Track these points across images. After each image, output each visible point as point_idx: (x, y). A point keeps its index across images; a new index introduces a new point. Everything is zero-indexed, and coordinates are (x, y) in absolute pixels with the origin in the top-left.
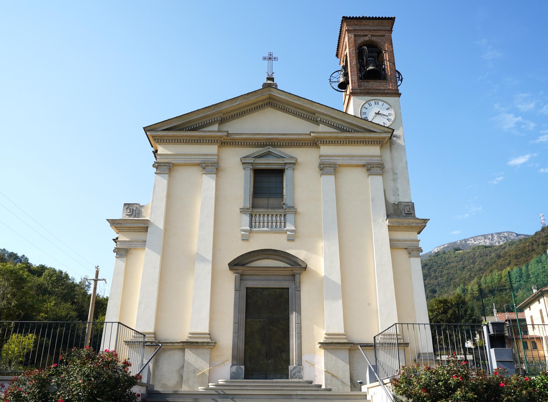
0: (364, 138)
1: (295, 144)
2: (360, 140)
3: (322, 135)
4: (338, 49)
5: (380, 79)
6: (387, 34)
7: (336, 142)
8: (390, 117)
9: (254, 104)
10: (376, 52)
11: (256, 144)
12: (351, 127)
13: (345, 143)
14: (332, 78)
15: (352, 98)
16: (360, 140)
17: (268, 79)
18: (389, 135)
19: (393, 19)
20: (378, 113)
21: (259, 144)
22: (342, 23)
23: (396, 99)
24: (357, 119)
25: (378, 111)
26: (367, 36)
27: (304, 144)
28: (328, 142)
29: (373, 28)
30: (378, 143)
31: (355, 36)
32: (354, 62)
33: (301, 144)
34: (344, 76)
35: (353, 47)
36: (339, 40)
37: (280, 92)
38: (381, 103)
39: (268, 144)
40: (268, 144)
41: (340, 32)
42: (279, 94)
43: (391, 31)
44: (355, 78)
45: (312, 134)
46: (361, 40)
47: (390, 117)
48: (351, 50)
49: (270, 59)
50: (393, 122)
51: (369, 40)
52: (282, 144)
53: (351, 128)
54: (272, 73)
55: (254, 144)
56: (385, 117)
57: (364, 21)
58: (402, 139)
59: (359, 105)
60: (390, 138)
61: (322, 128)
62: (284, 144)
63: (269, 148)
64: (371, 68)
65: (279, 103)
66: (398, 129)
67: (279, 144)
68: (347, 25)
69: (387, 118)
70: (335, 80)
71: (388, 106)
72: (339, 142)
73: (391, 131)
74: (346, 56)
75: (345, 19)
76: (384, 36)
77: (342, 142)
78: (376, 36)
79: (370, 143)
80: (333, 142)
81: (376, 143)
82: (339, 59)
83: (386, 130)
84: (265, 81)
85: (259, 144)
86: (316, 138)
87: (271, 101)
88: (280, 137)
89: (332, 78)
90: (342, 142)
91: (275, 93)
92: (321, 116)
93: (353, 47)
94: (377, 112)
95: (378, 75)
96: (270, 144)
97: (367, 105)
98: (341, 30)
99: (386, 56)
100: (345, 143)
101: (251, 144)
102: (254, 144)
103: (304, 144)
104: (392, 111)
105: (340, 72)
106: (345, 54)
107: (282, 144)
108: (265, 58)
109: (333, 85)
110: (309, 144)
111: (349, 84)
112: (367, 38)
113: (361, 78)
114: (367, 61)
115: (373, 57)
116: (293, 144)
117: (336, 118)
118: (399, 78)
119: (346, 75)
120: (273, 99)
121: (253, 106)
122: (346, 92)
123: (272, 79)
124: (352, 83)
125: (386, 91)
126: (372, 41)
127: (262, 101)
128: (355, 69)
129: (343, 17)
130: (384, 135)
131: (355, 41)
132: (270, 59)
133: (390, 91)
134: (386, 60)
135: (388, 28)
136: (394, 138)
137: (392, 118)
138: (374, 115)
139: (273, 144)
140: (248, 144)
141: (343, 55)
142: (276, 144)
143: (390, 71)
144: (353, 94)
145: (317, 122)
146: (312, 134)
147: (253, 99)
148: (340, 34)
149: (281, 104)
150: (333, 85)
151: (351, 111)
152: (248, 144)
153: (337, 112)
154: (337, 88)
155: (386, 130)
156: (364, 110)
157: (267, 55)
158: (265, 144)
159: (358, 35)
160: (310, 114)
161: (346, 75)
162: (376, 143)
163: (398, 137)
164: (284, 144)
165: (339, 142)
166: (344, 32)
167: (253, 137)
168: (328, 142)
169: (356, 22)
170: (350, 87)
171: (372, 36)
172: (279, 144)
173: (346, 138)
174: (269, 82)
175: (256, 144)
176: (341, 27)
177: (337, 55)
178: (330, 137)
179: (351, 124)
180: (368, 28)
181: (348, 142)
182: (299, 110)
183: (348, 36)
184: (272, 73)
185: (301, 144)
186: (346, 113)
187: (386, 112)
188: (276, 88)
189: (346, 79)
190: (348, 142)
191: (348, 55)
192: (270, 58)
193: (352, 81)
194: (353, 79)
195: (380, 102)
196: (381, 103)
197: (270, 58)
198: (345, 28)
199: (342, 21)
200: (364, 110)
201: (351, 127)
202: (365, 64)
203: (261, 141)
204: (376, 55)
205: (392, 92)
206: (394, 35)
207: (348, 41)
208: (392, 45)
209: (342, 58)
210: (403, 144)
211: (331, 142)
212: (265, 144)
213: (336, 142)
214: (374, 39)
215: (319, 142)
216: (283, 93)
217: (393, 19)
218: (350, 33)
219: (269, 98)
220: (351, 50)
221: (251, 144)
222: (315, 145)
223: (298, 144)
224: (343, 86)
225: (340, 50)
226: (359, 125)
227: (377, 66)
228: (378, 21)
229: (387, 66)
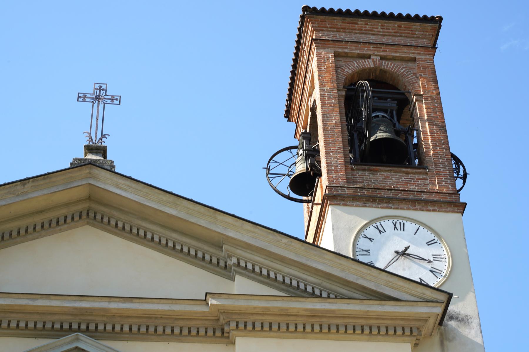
0: (366, 316)
1: (160, 330)
2: (352, 321)
3: (242, 303)
4: (290, 95)
5: (411, 165)
6: (421, 56)
7: (283, 328)
8: (436, 265)
9: (41, 211)
10: (393, 99)
11: (40, 326)
12: (326, 284)
13: (308, 329)
14: (272, 165)
15: (330, 210)
16: (352, 321)
17: (89, 149)
18: (438, 310)
19: (437, 21)
20: (404, 253)
21: (49, 326)
22: (302, 23)
23: (452, 217)
24: (343, 261)
25: (402, 245)
26: (369, 57)
27: (185, 332)
28: (258, 327)
29: (384, 40)
30: (408, 332)
31: (337, 55)
32: (336, 118)
33: (177, 331)
34: (308, 156)
35: (331, 81)
36: (293, 72)
37: (121, 181)
38: (410, 227)
39: (75, 326)
40: (75, 326)
41: (297, 48)
42: (118, 187)
43: (434, 47)
44: (339, 159)
45: (212, 301)
46: (353, 67)
47: (436, 265)
48: (326, 88)
49: (98, 98)
50: (448, 278)
51: (375, 69)
52: (118, 328)
53: (325, 288)
54: (103, 136)
55: (31, 325)
56: (425, 264)
57: (361, 23)
58: (475, 324)
59: (351, 230)
60: (441, 323)
61: (242, 285)
62: (126, 328)
63: (77, 339)
64: (380, 135)
65: (116, 214)
66: (462, 298)
67: (109, 328)
68: (315, 29)
69: (429, 266)
70: (284, 170)
71: (430, 236)
72: (292, 328)
73: (443, 297)
74: (313, 109)
75: (309, 13)
76: (414, 60)
77: (300, 328)
78: (394, 59)
79: (383, 331)
80: (275, 327)
81: (399, 332)
82: (293, 125)
83: (430, 294)
84: (81, 154)
85: (49, 326)
86: (223, 311)
87: (94, 206)
88: (113, 305)
89: (272, 165)
90: (300, 328)
91: (104, 182)
92: (239, 252)
93: (331, 81)
94: (401, 249)
95: (399, 153)
96: (83, 327)
97: (371, 231)
98: (298, 42)
99: (422, 110)
100: (308, 329)
101: (22, 325)
102: (31, 325)
103: (185, 332)
104: (441, 250)
105: (294, 151)
106: (310, 104)
107: (118, 328)
108: (85, 97)
109: (275, 182)
110: (202, 332)
111: (320, 175)
112: (369, 64)
113: (354, 162)
114: (369, 118)
115: (386, 111)
116: (152, 330)
117: (283, 260)
118: (458, 170)
119: (312, 154)
120: (100, 202)
121: (38, 219)
122: (311, 201)
123: (102, 151)
124: (329, 172)
125: (424, 197)
126: (384, 72)
127: (67, 204)
128: (338, 136)
129: (306, 9)
130: (423, 310)
131: (337, 68)
132: (98, 98)
133: (433, 197)
134: (421, 118)
135: (425, 42)
136: (453, 324)
137: (444, 266)
138: (391, 255)
139: (92, 327)
140: (13, 325)
141: (303, 111)
142: (101, 327)
143: (434, 145)
144: (332, 197)
145: (226, 270)
146: (212, 301)
147: (39, 197)
148: (296, 54)
149: (123, 217)
150: (275, 182)
151: (327, 241)
152: (13, 325)
153: (285, 240)
154: (287, 191)
155: (430, 294)
156: (363, 243)
157: (90, 90)
158: (66, 326)
159: (346, 55)
160: (206, 248)
161: (312, 154)
162: (399, 332)
163: (463, 320)
164: (126, 328)
165: (292, 328)
166: (306, 49)
167: (31, 303)
168: (258, 327)
169: (339, 22)
170: (324, 181)
171: (383, 58)
172: (109, 328)
173: (313, 315)
174: (90, 157)
175: (40, 326)
176: (299, 36)
177: (288, 114)
178: (265, 312)
179: (328, 276)
180: (372, 38)
181: (317, 328)
182: (174, 235)
183: (318, 56)
184: (103, 136)
185: (177, 331)
186: (314, 245)
187: (426, 252)
188: (111, 169)
189: (312, 165)
190: (317, 328)
191: (318, 103)
192: (99, 97)
193: (328, 165)
194: (333, 161)
195: (408, 225)
196: (410, 227)
197: (99, 97)
198: (310, 34)
199: (302, 17)
200: (363, 243)
201: (326, 284)
202: (364, 125)
203: (55, 318)
204: (394, 105)
205: (441, 198)
206: (440, 60)
207: (319, 67)
208: (436, 81)
209: (302, 118)
210: (479, 340)
211: (266, 327)
212: (66, 326)
213: (283, 328)
214: (387, 65)
215: (233, 325)
216: (128, 182)
217: (437, 21)
218: (324, 48)
219: (89, 198)
220: (326, 88)
221: (22, 325)
222: (218, 333)
223: (168, 331)
224: (303, 185)
225: (297, 98)
226: (351, 278)
227: (397, 133)
228: (397, 24)
229: (425, 133)
